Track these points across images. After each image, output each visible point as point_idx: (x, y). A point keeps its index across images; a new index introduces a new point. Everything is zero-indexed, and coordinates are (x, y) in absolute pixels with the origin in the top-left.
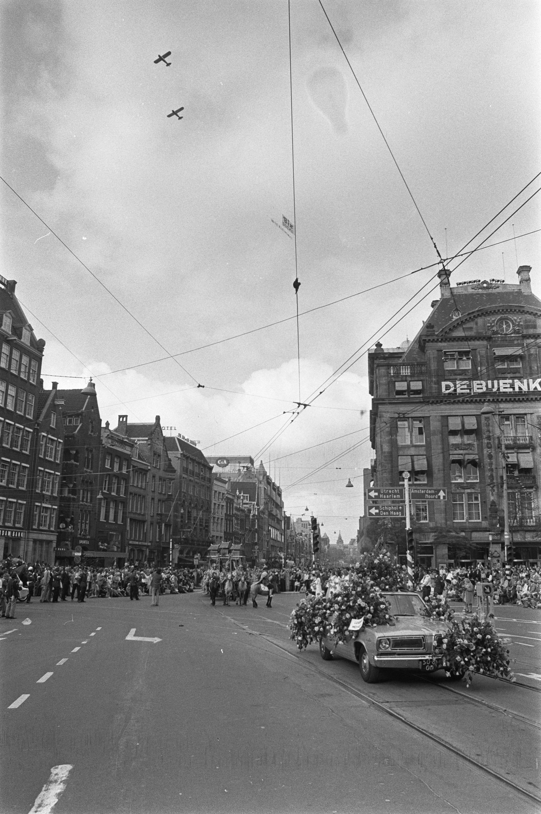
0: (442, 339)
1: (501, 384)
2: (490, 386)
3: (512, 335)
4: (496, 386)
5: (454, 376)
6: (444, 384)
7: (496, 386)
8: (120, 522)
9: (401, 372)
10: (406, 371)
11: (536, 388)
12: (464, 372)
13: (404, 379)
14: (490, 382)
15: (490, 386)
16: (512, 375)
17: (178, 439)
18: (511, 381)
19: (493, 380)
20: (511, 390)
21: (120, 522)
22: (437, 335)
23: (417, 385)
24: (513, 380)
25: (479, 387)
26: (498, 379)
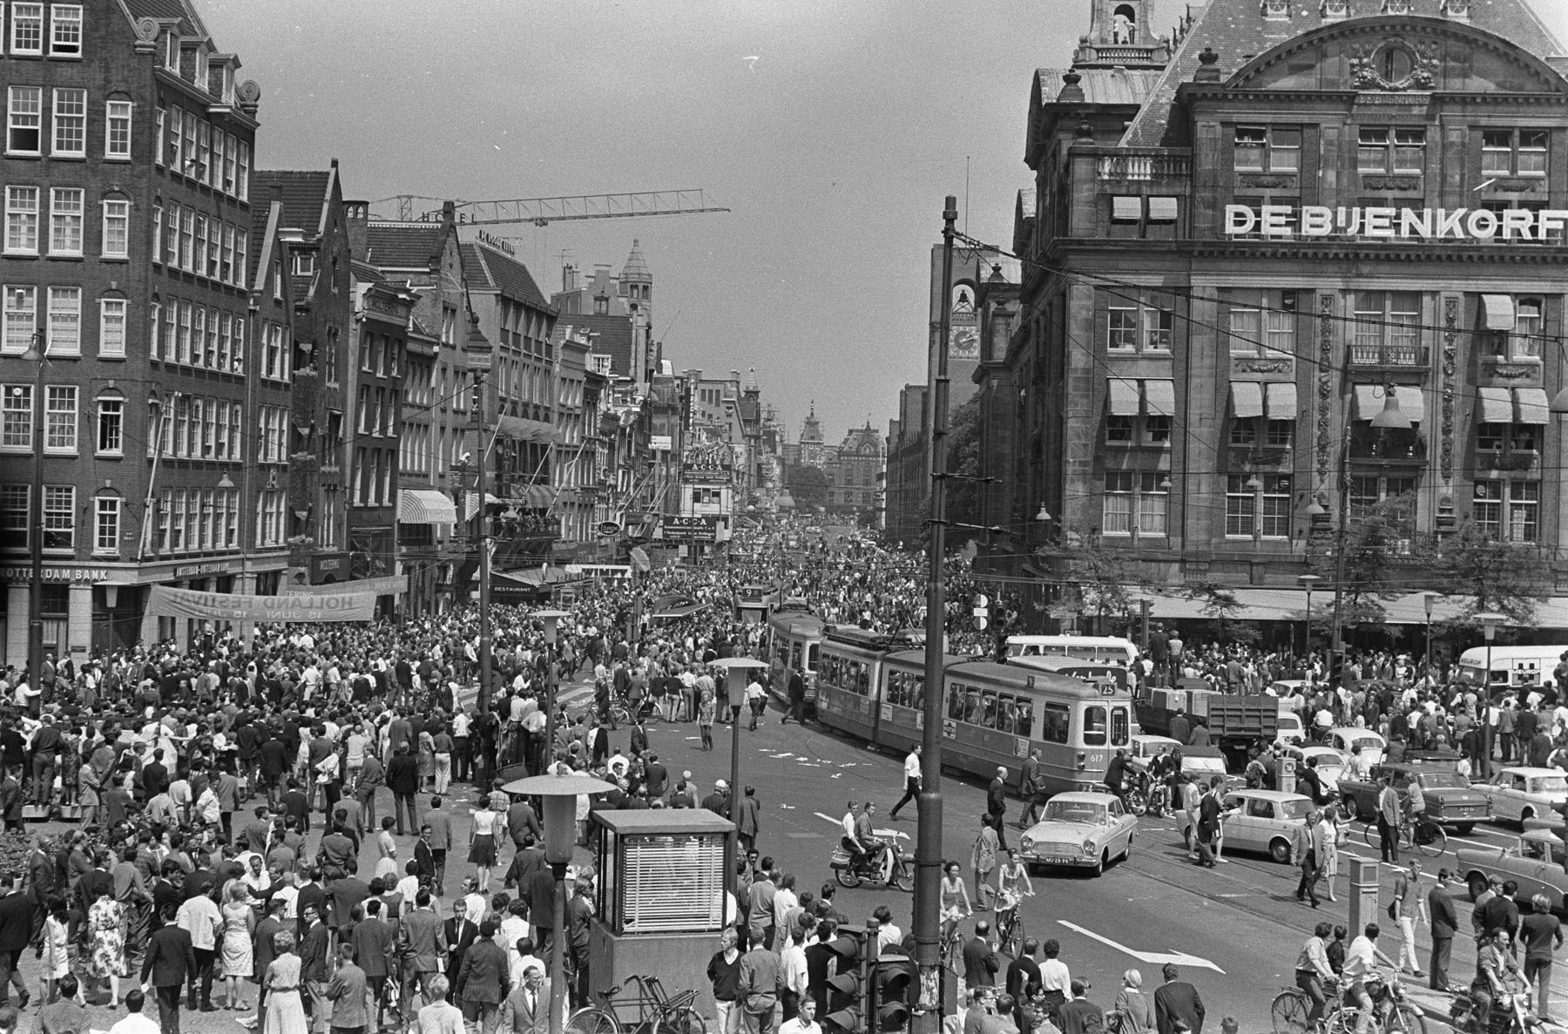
0: (1236, 96)
1: (1370, 221)
2: (1341, 222)
3: (1409, 92)
4: (1356, 220)
5: (1254, 193)
6: (1231, 210)
7: (1356, 220)
8: (386, 502)
9: (1130, 170)
10: (1140, 171)
11: (1451, 231)
12: (1281, 180)
13: (1135, 189)
14: (1342, 210)
15: (1341, 222)
16: (1398, 194)
17: (483, 249)
18: (1391, 211)
19: (1349, 206)
20: (1390, 233)
21: (386, 502)
22: (1223, 86)
23: (1166, 207)
24: (1399, 208)
25: (1318, 222)
26: (1364, 203)
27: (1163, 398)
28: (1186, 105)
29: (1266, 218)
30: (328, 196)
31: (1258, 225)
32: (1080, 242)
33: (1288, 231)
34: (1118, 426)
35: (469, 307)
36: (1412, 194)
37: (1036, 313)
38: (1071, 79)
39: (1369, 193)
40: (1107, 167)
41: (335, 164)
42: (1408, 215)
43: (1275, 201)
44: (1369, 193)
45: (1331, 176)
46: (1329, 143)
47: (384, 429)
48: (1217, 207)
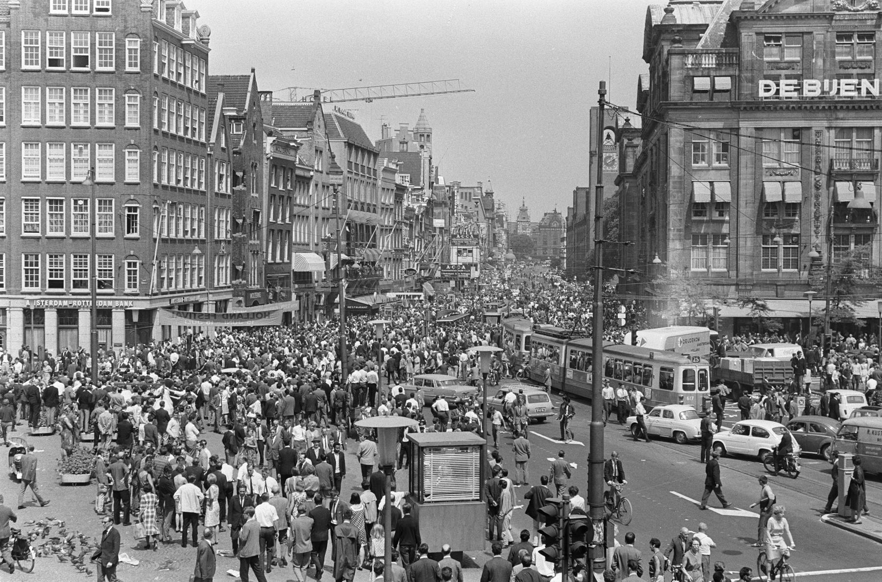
0: (764, 17)
1: (843, 87)
2: (826, 88)
3: (865, 12)
4: (835, 87)
6: (762, 83)
7: (835, 87)
8: (286, 260)
9: (703, 62)
10: (709, 62)
12: (791, 65)
14: (827, 82)
15: (826, 88)
18: (856, 81)
19: (831, 79)
20: (855, 94)
21: (286, 260)
22: (757, 12)
23: (724, 83)
24: (860, 79)
25: (812, 88)
26: (839, 77)
27: (723, 192)
28: (735, 23)
29: (783, 88)
30: (250, 89)
31: (778, 91)
32: (676, 104)
33: (795, 94)
34: (699, 209)
35: (330, 150)
36: (867, 71)
37: (650, 145)
38: (668, 11)
39: (842, 71)
40: (690, 60)
41: (253, 71)
42: (865, 83)
43: (788, 77)
44: (842, 71)
45: (820, 62)
46: (818, 43)
47: (283, 219)
48: (753, 81)
